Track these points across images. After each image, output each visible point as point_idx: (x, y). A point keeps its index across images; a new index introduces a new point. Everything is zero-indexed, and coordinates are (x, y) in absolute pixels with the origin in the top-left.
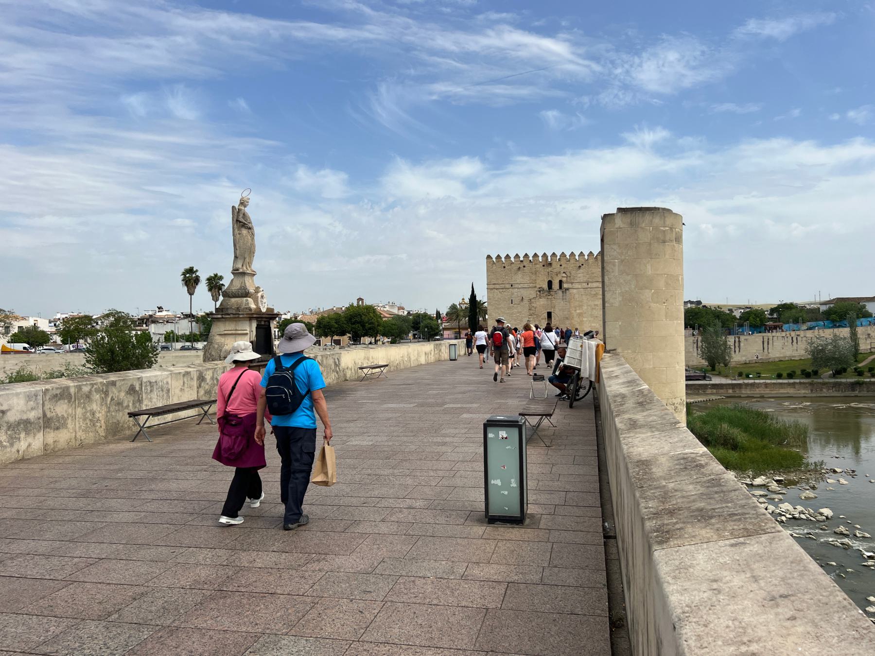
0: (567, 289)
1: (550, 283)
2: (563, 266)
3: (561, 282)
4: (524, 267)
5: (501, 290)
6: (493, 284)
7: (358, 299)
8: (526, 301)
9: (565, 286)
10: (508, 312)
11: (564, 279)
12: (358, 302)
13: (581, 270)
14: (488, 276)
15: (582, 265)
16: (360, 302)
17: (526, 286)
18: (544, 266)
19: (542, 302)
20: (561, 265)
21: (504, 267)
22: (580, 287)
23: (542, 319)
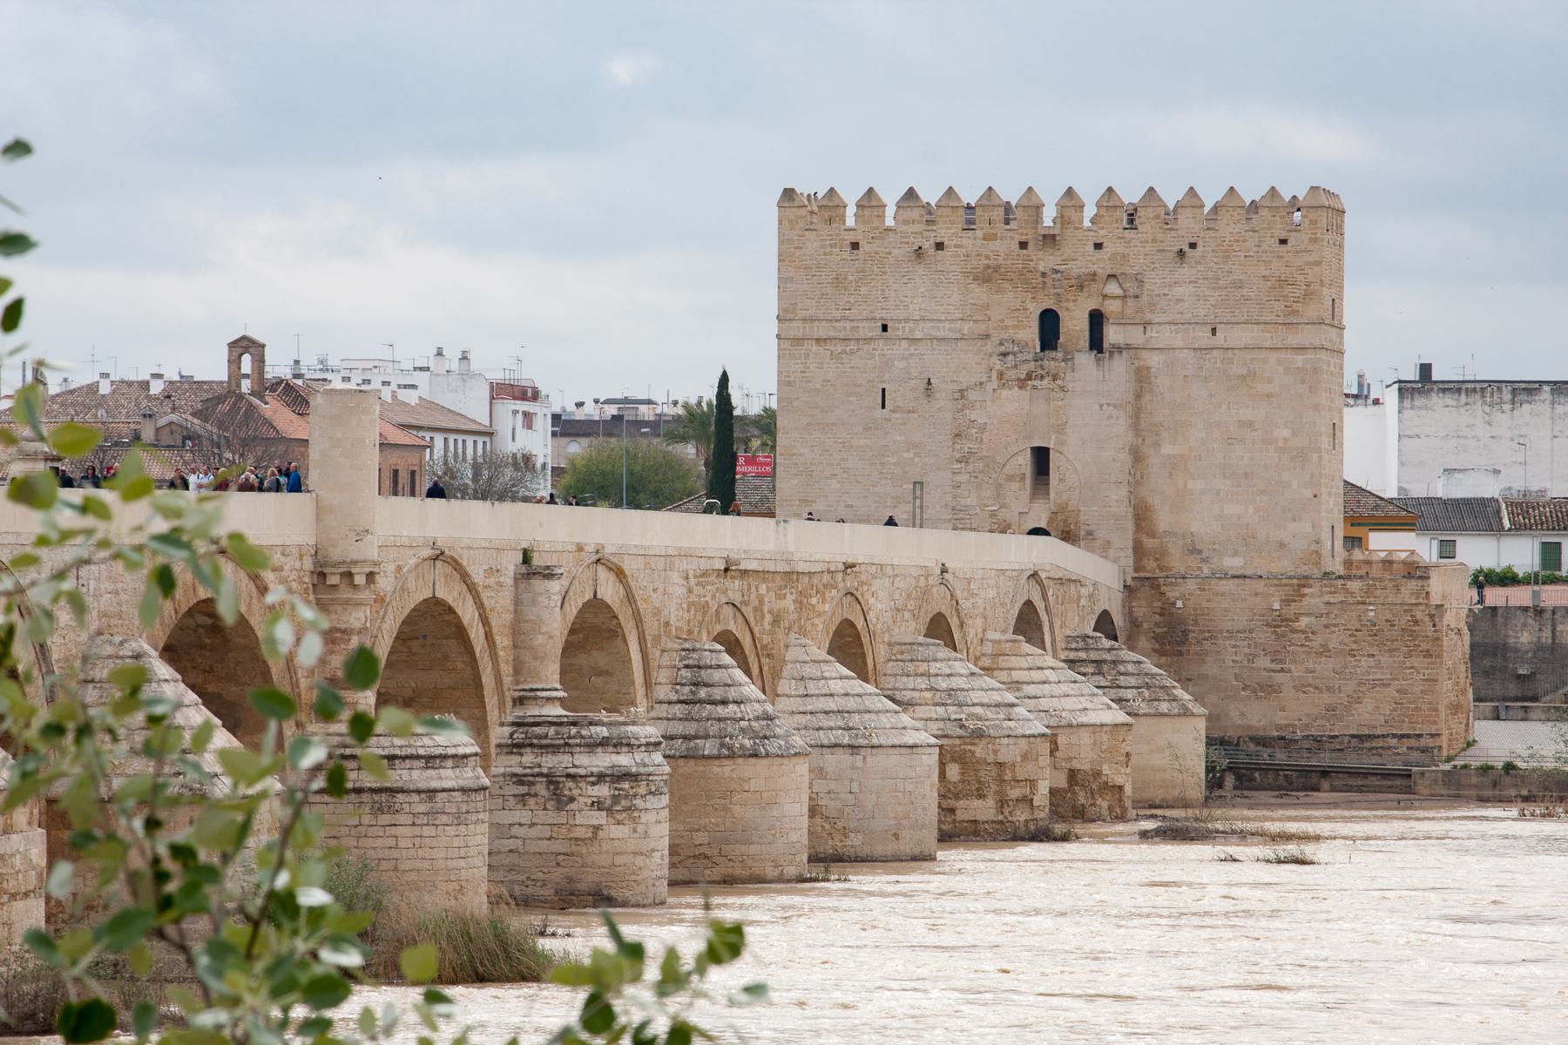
0: (1119, 349)
1: (1049, 325)
2: (1109, 248)
3: (1097, 320)
4: (940, 246)
5: (839, 348)
6: (805, 320)
7: (233, 345)
8: (943, 400)
9: (1112, 335)
10: (863, 442)
11: (1111, 307)
12: (235, 362)
13: (1186, 272)
14: (783, 281)
15: (1193, 246)
16: (246, 360)
17: (944, 330)
18: (1023, 245)
19: (1013, 401)
20: (1098, 246)
21: (855, 246)
22: (1178, 343)
23: (1010, 478)
